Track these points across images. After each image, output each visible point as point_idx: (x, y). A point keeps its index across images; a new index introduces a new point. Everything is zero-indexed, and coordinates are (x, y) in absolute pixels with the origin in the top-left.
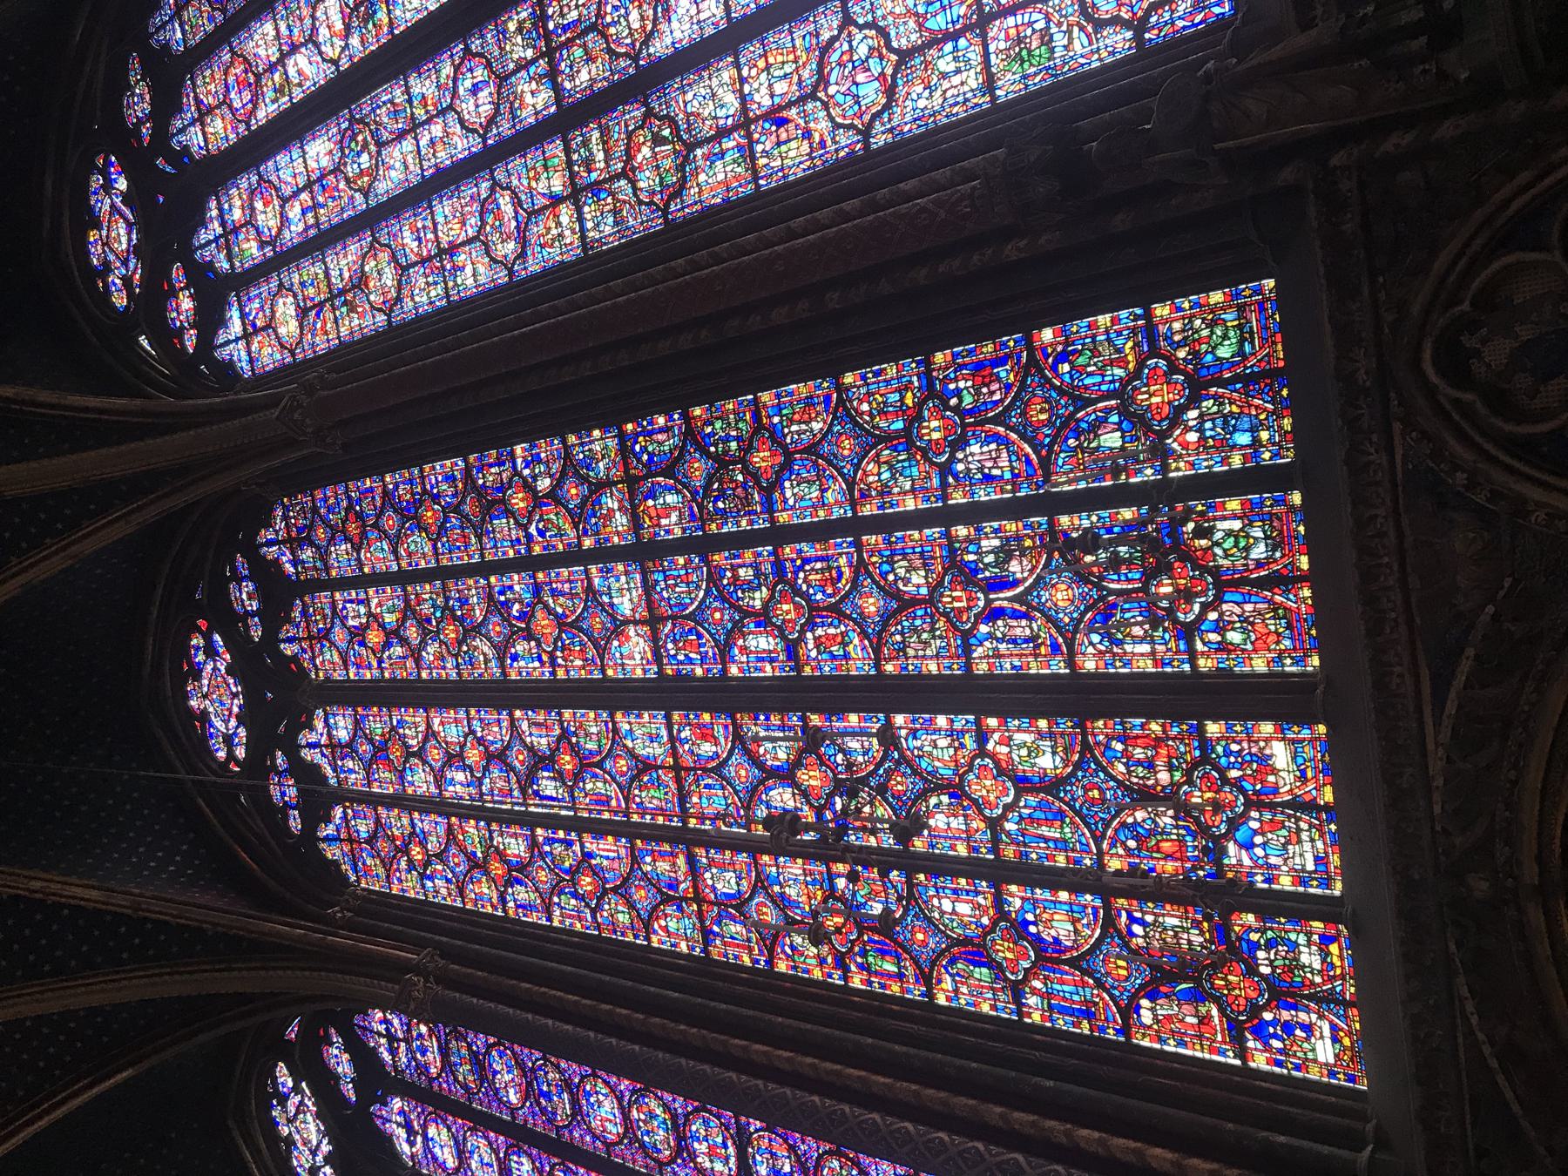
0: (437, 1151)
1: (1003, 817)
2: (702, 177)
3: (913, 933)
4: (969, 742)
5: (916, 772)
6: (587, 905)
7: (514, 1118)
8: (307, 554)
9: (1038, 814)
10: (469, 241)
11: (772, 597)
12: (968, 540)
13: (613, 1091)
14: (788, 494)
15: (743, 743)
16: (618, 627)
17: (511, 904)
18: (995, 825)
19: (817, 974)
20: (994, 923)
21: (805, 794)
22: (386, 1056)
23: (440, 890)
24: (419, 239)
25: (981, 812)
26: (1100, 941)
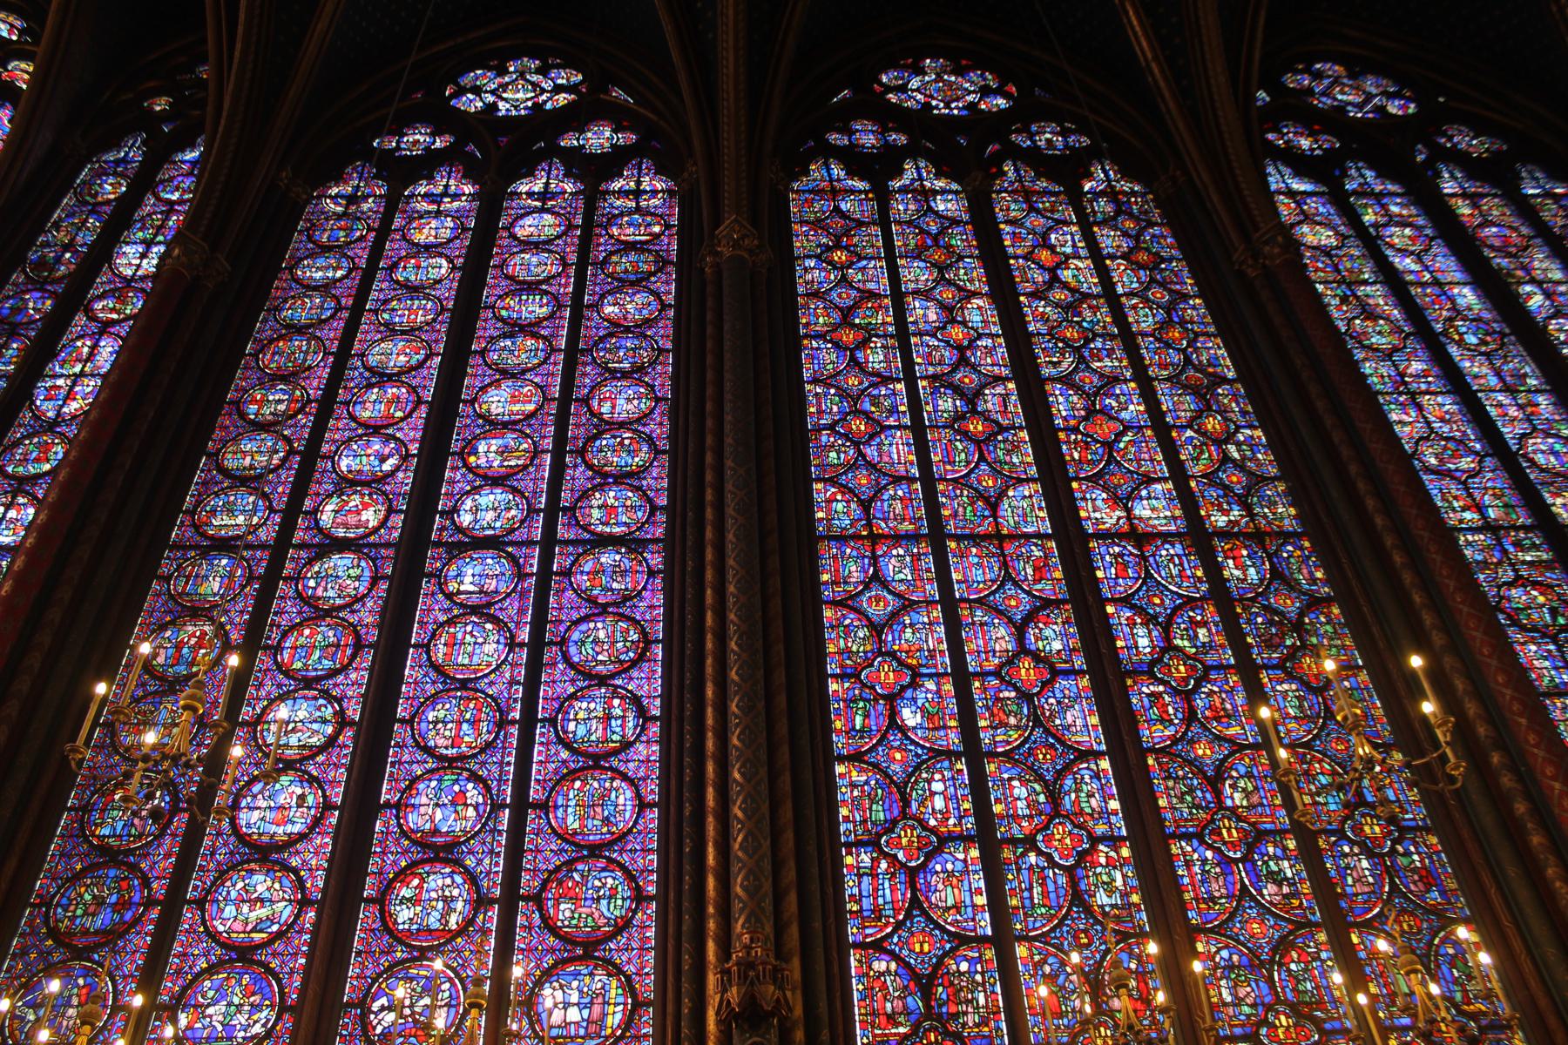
0: (528, 221)
1: (1040, 853)
2: (1533, 648)
3: (899, 749)
4: (1101, 829)
5: (1060, 775)
6: (835, 423)
7: (589, 306)
8: (1103, 206)
9: (1051, 887)
10: (1428, 423)
11: (1189, 657)
12: (1285, 849)
13: (646, 416)
14: (1286, 686)
15: (1043, 608)
16: (1121, 501)
17: (815, 344)
18: (1029, 843)
19: (831, 648)
20: (933, 831)
21: (1011, 661)
22: (617, 185)
23: (812, 274)
24: (1417, 376)
25: (1038, 831)
26: (943, 930)
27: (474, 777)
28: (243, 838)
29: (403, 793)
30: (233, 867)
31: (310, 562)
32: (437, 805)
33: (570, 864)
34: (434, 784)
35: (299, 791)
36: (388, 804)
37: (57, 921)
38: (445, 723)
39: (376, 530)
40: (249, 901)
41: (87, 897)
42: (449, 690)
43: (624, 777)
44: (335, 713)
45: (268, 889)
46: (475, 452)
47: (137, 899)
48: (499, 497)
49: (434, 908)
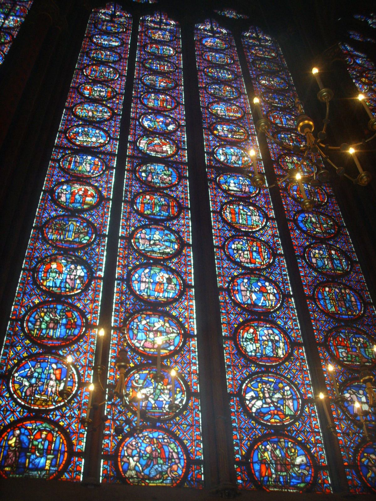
27: (267, 279)
28: (139, 298)
29: (229, 283)
30: (138, 312)
31: (140, 165)
32: (251, 292)
33: (337, 330)
34: (246, 281)
35: (167, 276)
36: (221, 288)
37: (30, 330)
38: (243, 251)
39: (172, 156)
40: (152, 331)
41: (47, 319)
42: (239, 236)
43: (350, 288)
44: (177, 239)
45: (163, 326)
46: (217, 130)
47: (79, 322)
48: (236, 151)
49: (267, 345)
